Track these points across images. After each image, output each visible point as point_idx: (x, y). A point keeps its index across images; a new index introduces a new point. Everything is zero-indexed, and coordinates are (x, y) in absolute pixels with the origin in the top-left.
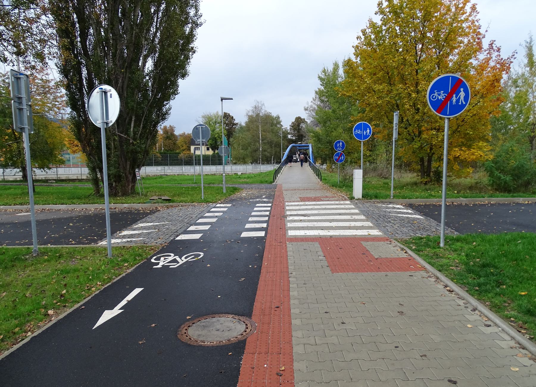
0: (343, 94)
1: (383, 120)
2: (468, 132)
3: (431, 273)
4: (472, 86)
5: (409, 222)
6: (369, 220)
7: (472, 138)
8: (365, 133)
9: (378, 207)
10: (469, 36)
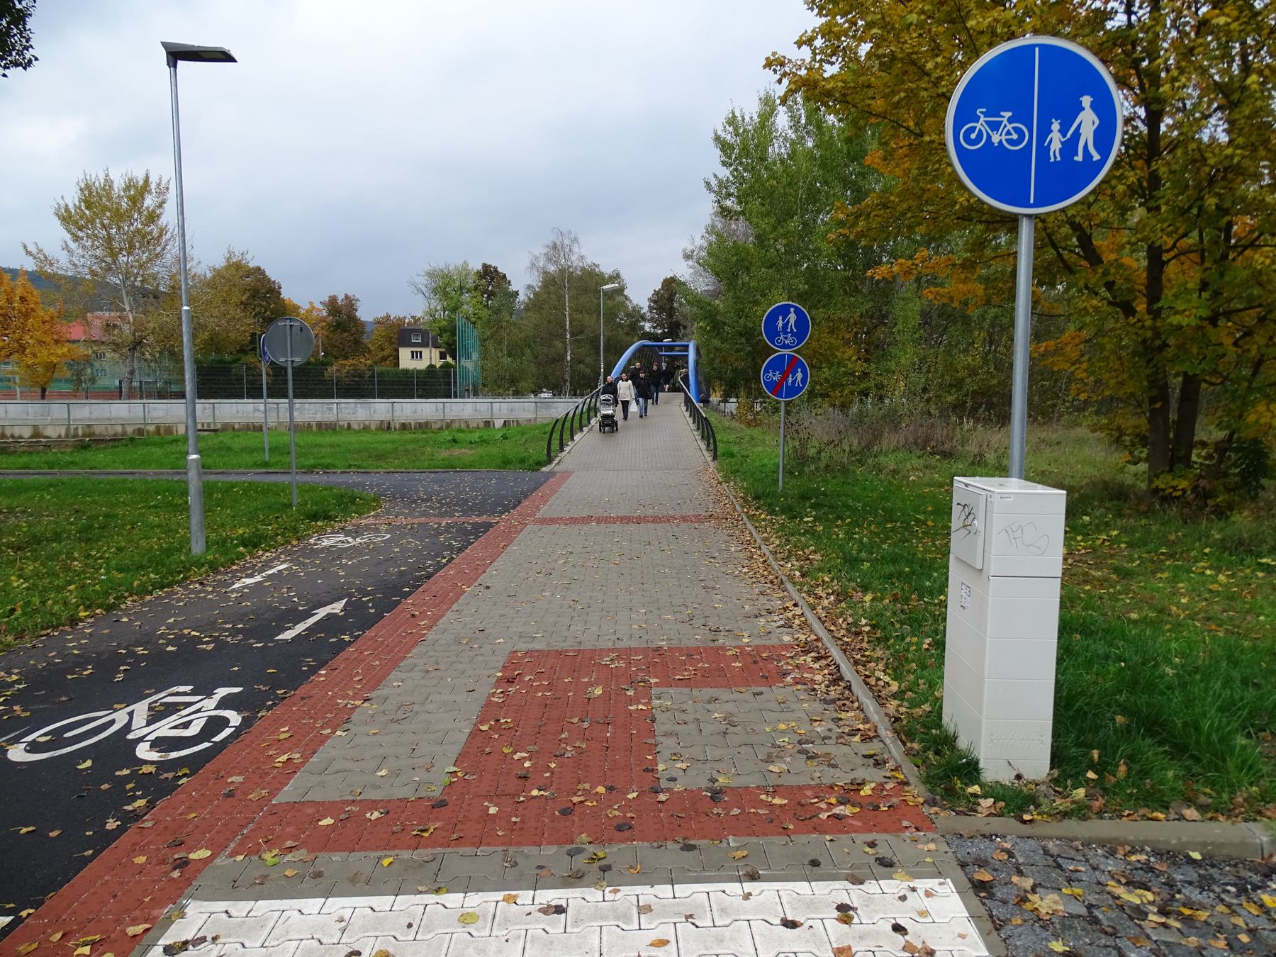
8: (1056, 141)
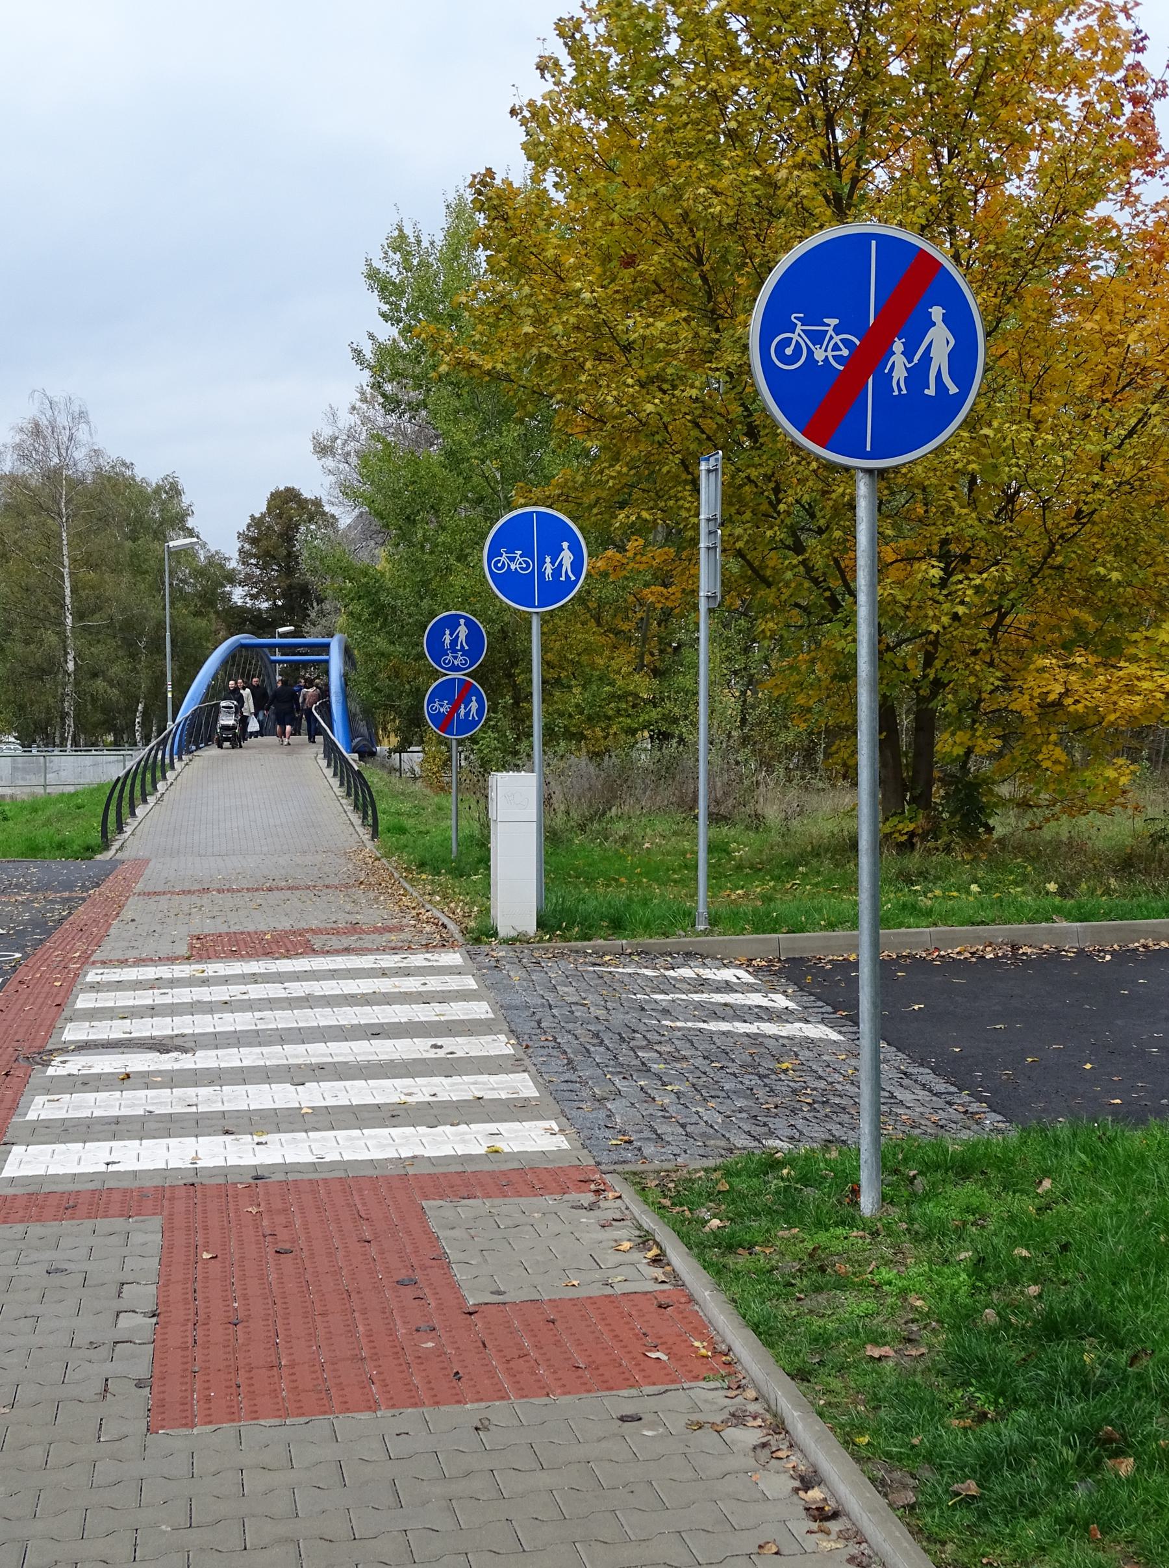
0: (459, 362)
1: (672, 503)
2: (1102, 571)
3: (751, 1394)
4: (1111, 334)
5: (750, 1067)
6: (527, 1062)
7: (1125, 604)
8: (549, 569)
9: (608, 982)
10: (1090, 81)
